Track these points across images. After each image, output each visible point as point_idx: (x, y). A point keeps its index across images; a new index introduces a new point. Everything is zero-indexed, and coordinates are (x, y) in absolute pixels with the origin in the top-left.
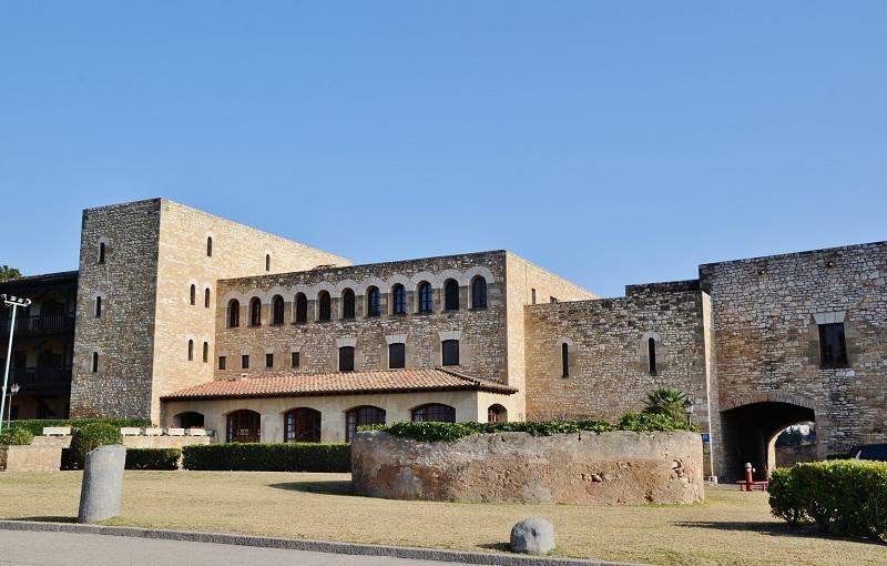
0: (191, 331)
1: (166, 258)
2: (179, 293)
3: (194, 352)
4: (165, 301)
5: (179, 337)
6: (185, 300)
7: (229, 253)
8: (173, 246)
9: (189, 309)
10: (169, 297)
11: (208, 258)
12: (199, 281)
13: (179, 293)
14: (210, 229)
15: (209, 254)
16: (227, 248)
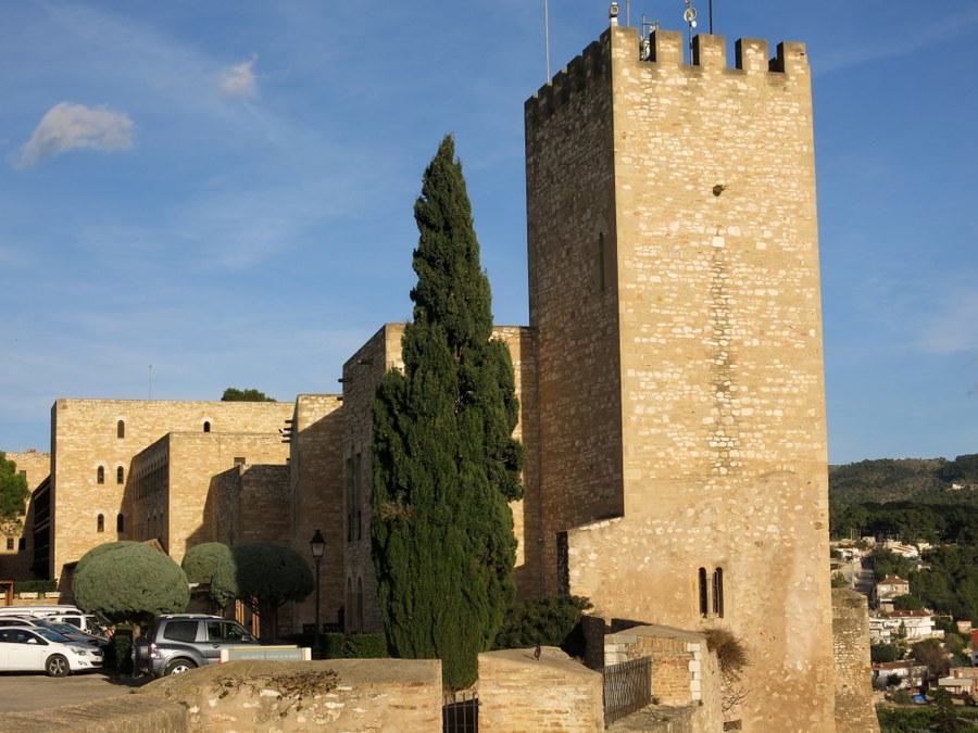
0: (101, 507)
1: (66, 449)
2: (83, 476)
3: (105, 525)
4: (66, 485)
5: (83, 512)
6: (90, 481)
7: (148, 430)
8: (73, 437)
9: (96, 488)
10: (70, 481)
11: (121, 441)
12: (108, 461)
13: (83, 476)
14: (121, 414)
15: (121, 433)
16: (145, 427)
